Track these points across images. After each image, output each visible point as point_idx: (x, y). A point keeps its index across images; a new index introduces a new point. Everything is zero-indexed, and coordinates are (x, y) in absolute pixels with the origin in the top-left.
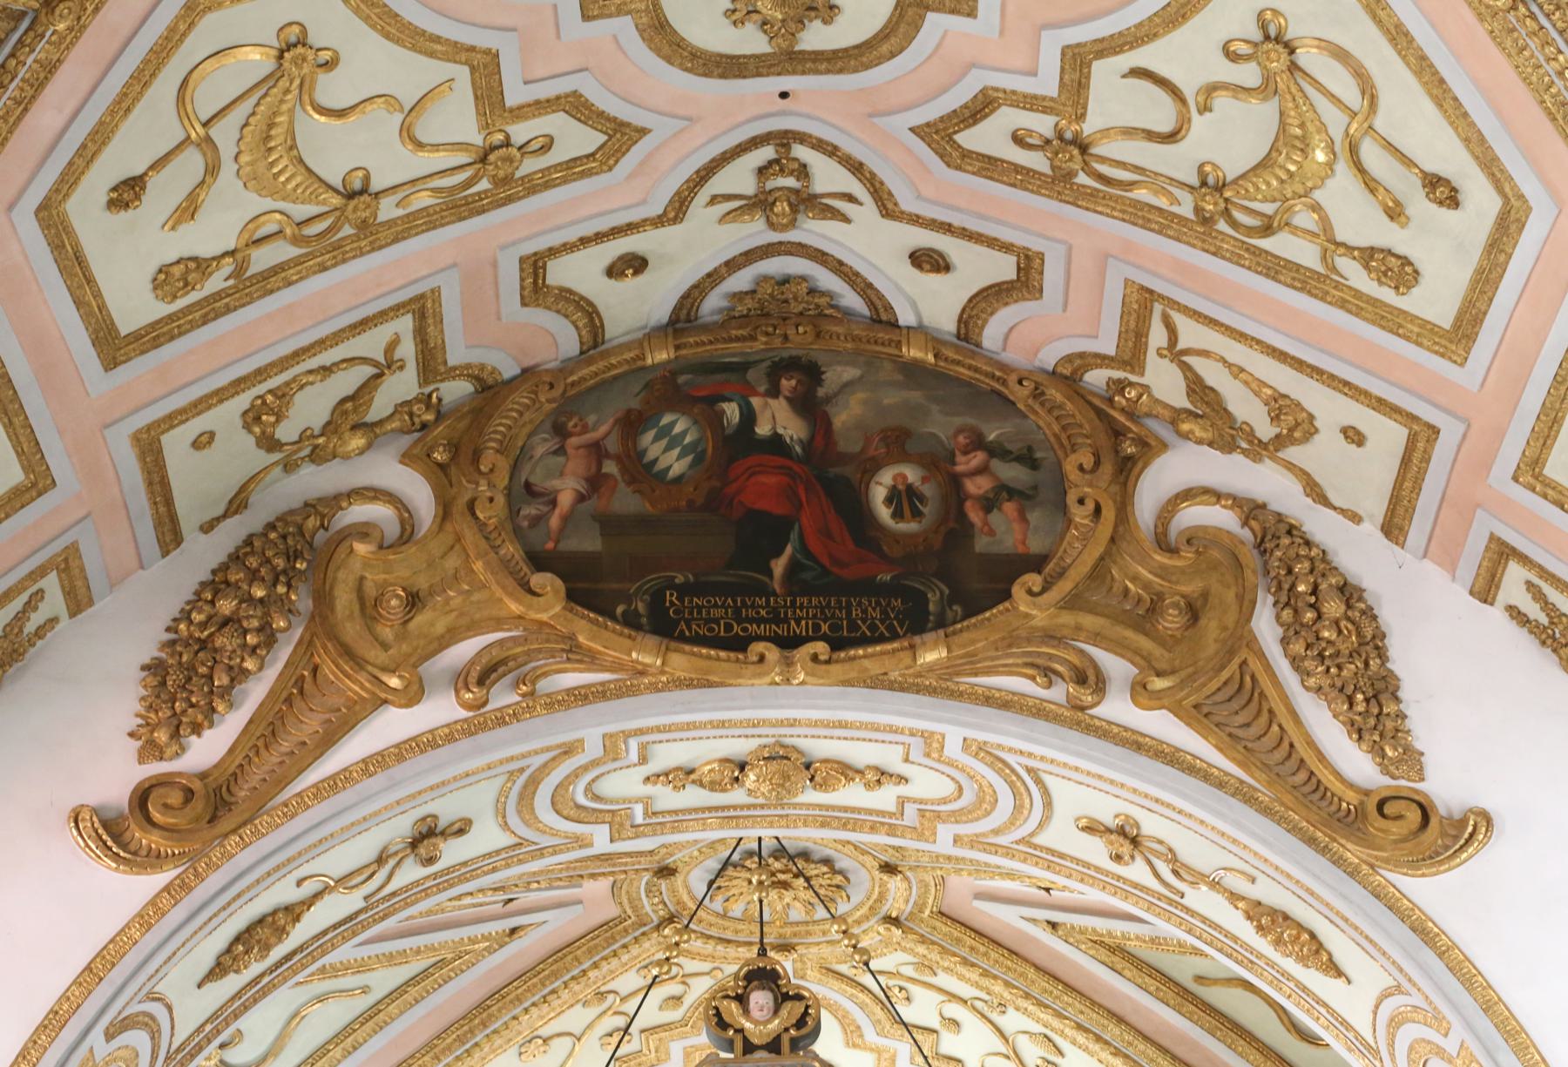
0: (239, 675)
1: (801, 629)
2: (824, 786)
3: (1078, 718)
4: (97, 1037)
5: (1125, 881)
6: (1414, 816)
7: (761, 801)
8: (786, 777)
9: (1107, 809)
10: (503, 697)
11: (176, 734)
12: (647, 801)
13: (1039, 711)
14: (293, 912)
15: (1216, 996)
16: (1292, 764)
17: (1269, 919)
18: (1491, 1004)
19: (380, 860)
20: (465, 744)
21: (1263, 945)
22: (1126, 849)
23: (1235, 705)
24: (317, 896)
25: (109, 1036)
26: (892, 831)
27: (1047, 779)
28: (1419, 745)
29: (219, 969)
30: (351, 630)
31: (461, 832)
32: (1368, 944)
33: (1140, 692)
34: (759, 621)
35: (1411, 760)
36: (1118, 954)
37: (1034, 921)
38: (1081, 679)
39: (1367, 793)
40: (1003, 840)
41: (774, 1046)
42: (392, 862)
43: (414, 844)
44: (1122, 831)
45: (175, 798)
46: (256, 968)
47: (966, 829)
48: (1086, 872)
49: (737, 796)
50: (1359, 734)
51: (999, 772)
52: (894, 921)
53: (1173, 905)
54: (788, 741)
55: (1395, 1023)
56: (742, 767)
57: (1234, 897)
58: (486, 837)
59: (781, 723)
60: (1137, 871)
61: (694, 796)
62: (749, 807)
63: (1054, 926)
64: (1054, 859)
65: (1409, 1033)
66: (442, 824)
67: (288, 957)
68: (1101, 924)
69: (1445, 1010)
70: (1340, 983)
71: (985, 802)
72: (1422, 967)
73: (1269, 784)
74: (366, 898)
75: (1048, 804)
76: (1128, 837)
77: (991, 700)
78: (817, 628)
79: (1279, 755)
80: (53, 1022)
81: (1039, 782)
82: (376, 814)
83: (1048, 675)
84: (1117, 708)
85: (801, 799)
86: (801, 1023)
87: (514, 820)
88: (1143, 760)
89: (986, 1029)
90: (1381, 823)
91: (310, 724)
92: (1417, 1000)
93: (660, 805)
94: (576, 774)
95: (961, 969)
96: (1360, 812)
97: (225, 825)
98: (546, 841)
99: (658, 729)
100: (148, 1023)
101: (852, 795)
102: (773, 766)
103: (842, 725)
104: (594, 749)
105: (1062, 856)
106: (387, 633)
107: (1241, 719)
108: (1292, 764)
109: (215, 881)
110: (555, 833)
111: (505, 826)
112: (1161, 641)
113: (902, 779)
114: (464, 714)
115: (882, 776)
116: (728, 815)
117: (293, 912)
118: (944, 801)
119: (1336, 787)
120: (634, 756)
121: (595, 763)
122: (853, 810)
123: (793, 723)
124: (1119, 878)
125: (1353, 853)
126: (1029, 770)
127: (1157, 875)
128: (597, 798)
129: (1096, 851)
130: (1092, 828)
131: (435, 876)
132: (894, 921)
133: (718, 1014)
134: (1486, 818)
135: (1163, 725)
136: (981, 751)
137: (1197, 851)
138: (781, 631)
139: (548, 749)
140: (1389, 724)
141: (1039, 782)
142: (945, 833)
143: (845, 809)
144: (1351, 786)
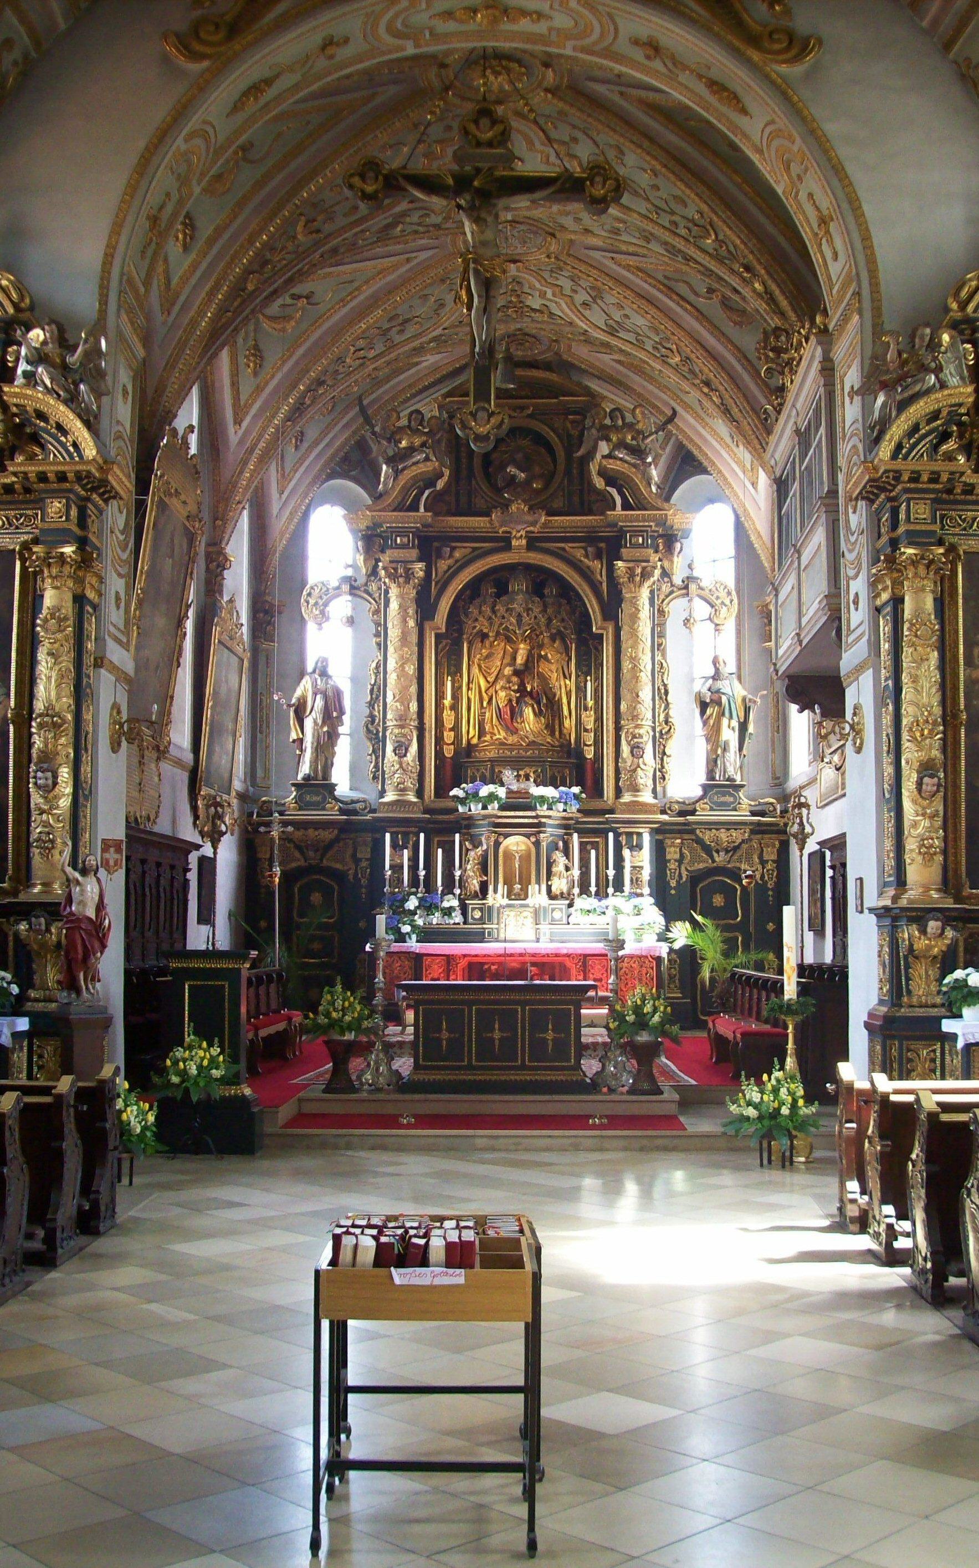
2: (514, 21)
22: (652, 53)
27: (618, 20)
37: (612, 91)
40: (596, 48)
41: (490, 144)
43: (324, 48)
47: (579, 43)
49: (472, 26)
57: (700, 77)
60: (657, 65)
63: (622, 94)
68: (643, 94)
75: (616, 30)
86: (503, 133)
89: (590, 142)
94: (397, 15)
101: (525, 25)
102: (490, 11)
117: (268, 82)
121: (406, 9)
125: (756, 56)
127: (666, 65)
128: (407, 26)
129: (638, 55)
130: (636, 42)
132: (547, 90)
133: (465, 128)
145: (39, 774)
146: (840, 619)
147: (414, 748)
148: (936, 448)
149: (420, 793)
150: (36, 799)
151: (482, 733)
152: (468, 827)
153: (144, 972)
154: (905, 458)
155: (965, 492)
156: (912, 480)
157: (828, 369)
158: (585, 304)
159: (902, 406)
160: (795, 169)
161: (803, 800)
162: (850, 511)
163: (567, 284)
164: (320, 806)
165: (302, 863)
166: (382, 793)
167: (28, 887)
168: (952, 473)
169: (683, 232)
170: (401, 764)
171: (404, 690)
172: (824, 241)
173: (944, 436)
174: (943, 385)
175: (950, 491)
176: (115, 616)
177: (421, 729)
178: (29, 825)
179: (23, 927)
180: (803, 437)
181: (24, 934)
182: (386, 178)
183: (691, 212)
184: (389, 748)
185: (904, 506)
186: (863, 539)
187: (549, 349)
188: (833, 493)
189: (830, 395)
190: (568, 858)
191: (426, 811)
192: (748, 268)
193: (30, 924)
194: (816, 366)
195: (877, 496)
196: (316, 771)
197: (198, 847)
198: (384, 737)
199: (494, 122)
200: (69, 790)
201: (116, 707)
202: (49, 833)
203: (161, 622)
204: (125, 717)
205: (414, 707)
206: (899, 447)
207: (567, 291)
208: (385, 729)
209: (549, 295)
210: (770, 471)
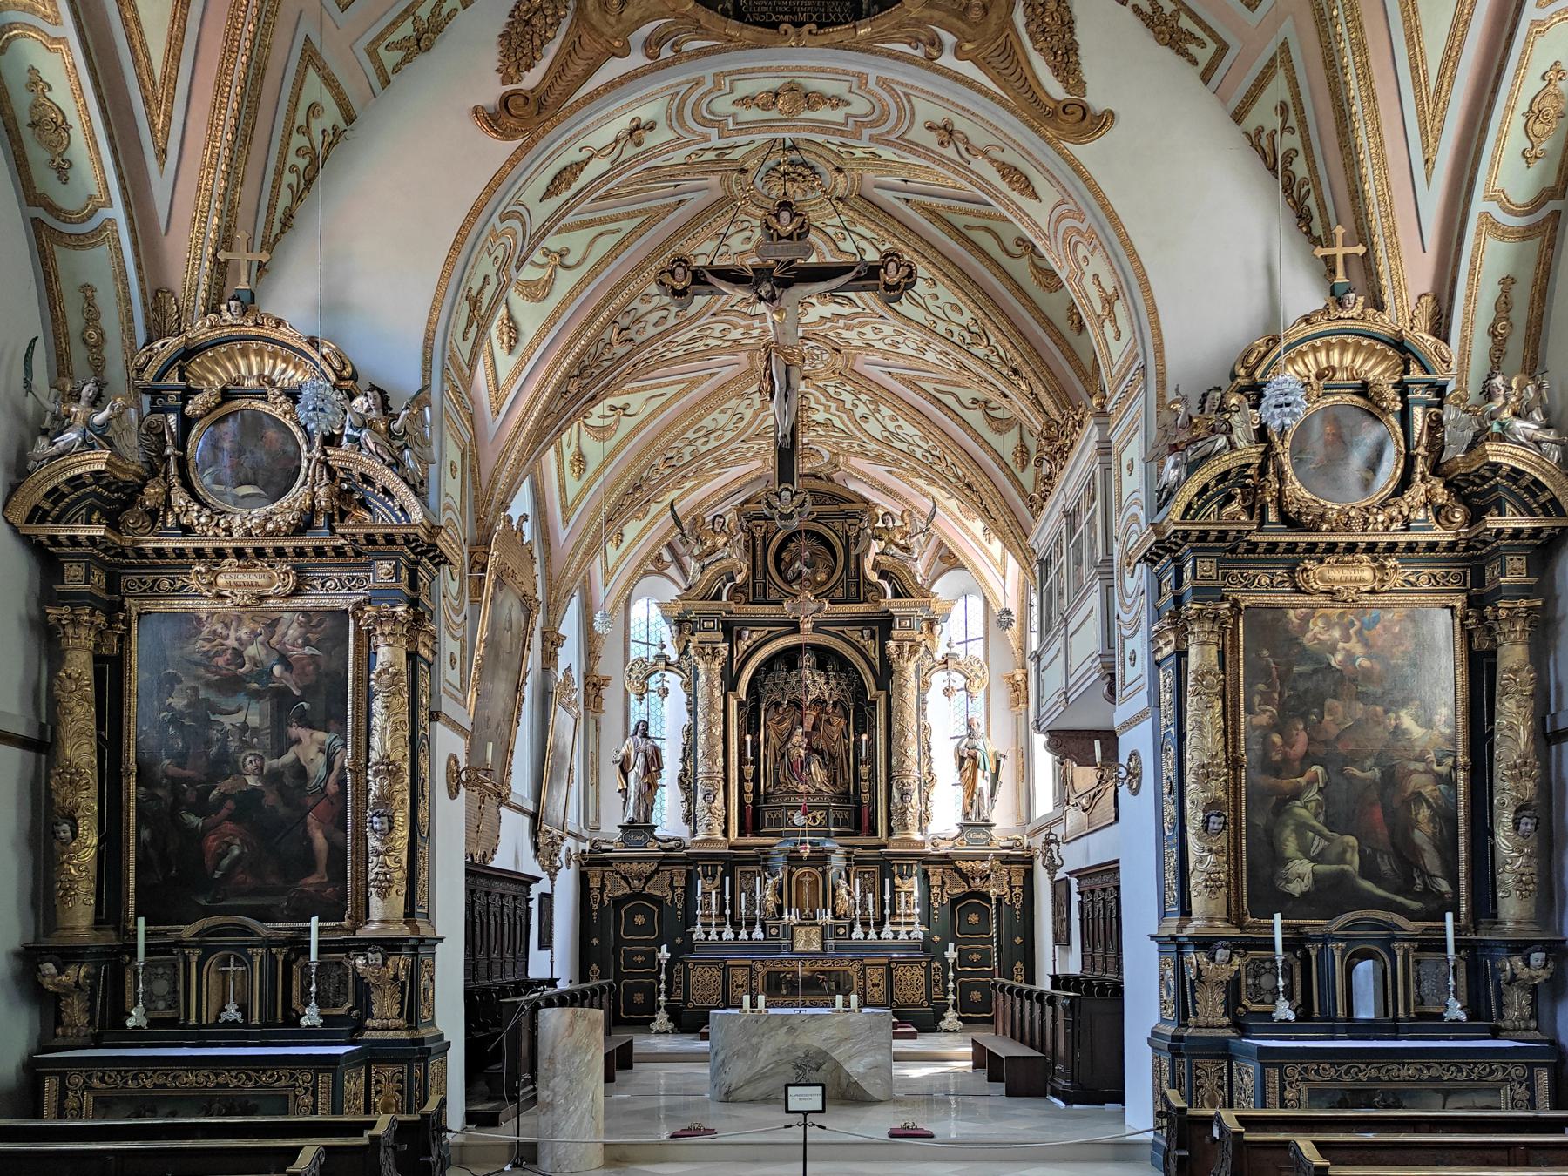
0: (545, 41)
1: (804, 18)
2: (812, 107)
3: (929, 63)
4: (495, 219)
5: (944, 157)
6: (1079, 113)
7: (784, 117)
8: (796, 101)
9: (938, 115)
10: (666, 53)
11: (518, 70)
12: (734, 116)
13: (911, 61)
14: (580, 166)
15: (973, 235)
16: (1026, 88)
17: (1008, 171)
18: (1105, 205)
19: (617, 141)
20: (650, 77)
21: (1003, 186)
23: (1002, 58)
24: (590, 158)
25: (502, 221)
26: (842, 134)
28: (1084, 79)
29: (548, 194)
30: (595, 17)
31: (652, 128)
32: (1052, 179)
33: (958, 53)
34: (784, 13)
35: (1081, 85)
36: (932, 213)
38: (933, 45)
39: (1059, 102)
40: (891, 137)
42: (622, 143)
43: (631, 133)
44: (945, 127)
45: (521, 101)
46: (566, 195)
48: (925, 152)
49: (773, 114)
50: (1056, 71)
51: (892, 96)
52: (839, 199)
53: (963, 168)
54: (797, 80)
55: (1059, 220)
56: (777, 95)
58: (662, 135)
59: (794, 69)
60: (950, 152)
61: (753, 114)
62: (780, 120)
64: (913, 147)
65: (1066, 223)
66: (643, 122)
67: (580, 191)
69: (1085, 210)
70: (1035, 202)
71: (885, 114)
72: (1077, 189)
73: (1014, 99)
74: (612, 163)
75: (913, 115)
76: (947, 132)
77: (891, 55)
78: (811, 17)
79: (1020, 83)
80: (476, 211)
81: (909, 101)
82: (612, 113)
83: (914, 41)
84: (947, 60)
85: (803, 116)
87: (675, 123)
88: (958, 87)
90: (1064, 117)
91: (579, 66)
92: (1071, 206)
93: (740, 119)
95: (866, 223)
96: (1055, 113)
97: (543, 117)
98: (691, 137)
99: (738, 72)
100: (519, 216)
101: (824, 113)
103: (822, 70)
104: (709, 84)
105: (917, 145)
106: (612, 20)
107: (1003, 65)
108: (1026, 88)
109: (541, 144)
110: (690, 131)
111: (671, 127)
112: (969, 25)
113: (848, 103)
114: (650, 62)
115: (838, 102)
116: (769, 125)
117: (580, 166)
118: (866, 116)
119: (1045, 99)
120: (728, 90)
121: (710, 92)
122: (827, 122)
123: (800, 69)
124: (941, 156)
126: (907, 95)
129: (931, 140)
131: (642, 153)
134: (1112, 114)
135: (967, 69)
136: (883, 83)
137: (979, 138)
138: (794, 18)
139: (688, 82)
140: (1072, 67)
141: (909, 101)
142: (866, 133)
143: (822, 122)
144: (1052, 99)
145: (375, 819)
146: (1113, 676)
147: (721, 795)
148: (1221, 507)
149: (726, 833)
150: (374, 843)
151: (777, 783)
152: (766, 860)
153: (486, 991)
154: (1193, 518)
155: (1247, 551)
156: (1199, 539)
157: (1104, 448)
158: (864, 418)
159: (1192, 467)
160: (1082, 251)
161: (1052, 837)
162: (1127, 576)
163: (848, 398)
164: (639, 844)
165: (627, 891)
166: (694, 833)
167: (367, 923)
168: (1239, 531)
169: (956, 339)
170: (710, 809)
171: (712, 747)
172: (1107, 322)
173: (1229, 499)
174: (1232, 446)
175: (1233, 551)
176: (452, 675)
177: (726, 780)
178: (367, 867)
179: (360, 961)
180: (1071, 516)
181: (360, 969)
182: (694, 273)
183: (966, 318)
184: (700, 797)
185: (1189, 565)
186: (1144, 600)
187: (830, 462)
188: (1108, 559)
189: (1106, 471)
190: (849, 884)
191: (730, 848)
192: (1016, 372)
193: (367, 959)
194: (1092, 446)
195: (1161, 557)
196: (639, 814)
197: (537, 880)
198: (695, 786)
199: (793, 215)
200: (406, 833)
201: (453, 758)
202: (385, 874)
203: (502, 687)
204: (463, 765)
205: (720, 761)
206: (1189, 507)
207: (848, 405)
208: (696, 780)
209: (833, 410)
210: (1026, 556)
